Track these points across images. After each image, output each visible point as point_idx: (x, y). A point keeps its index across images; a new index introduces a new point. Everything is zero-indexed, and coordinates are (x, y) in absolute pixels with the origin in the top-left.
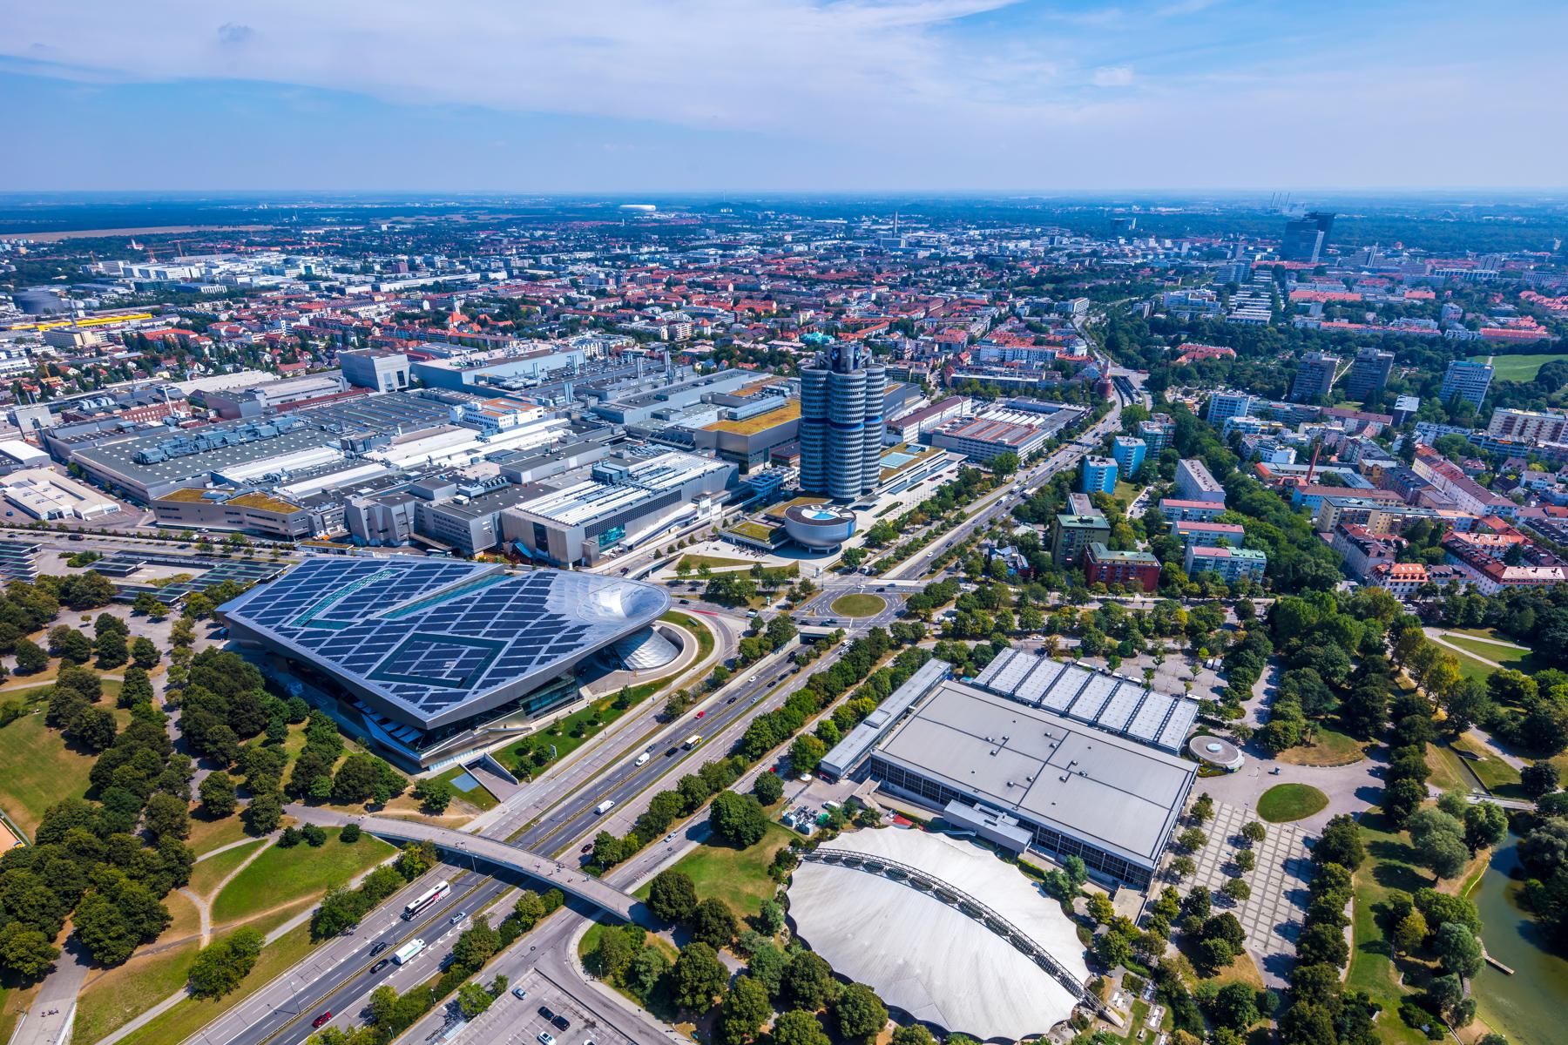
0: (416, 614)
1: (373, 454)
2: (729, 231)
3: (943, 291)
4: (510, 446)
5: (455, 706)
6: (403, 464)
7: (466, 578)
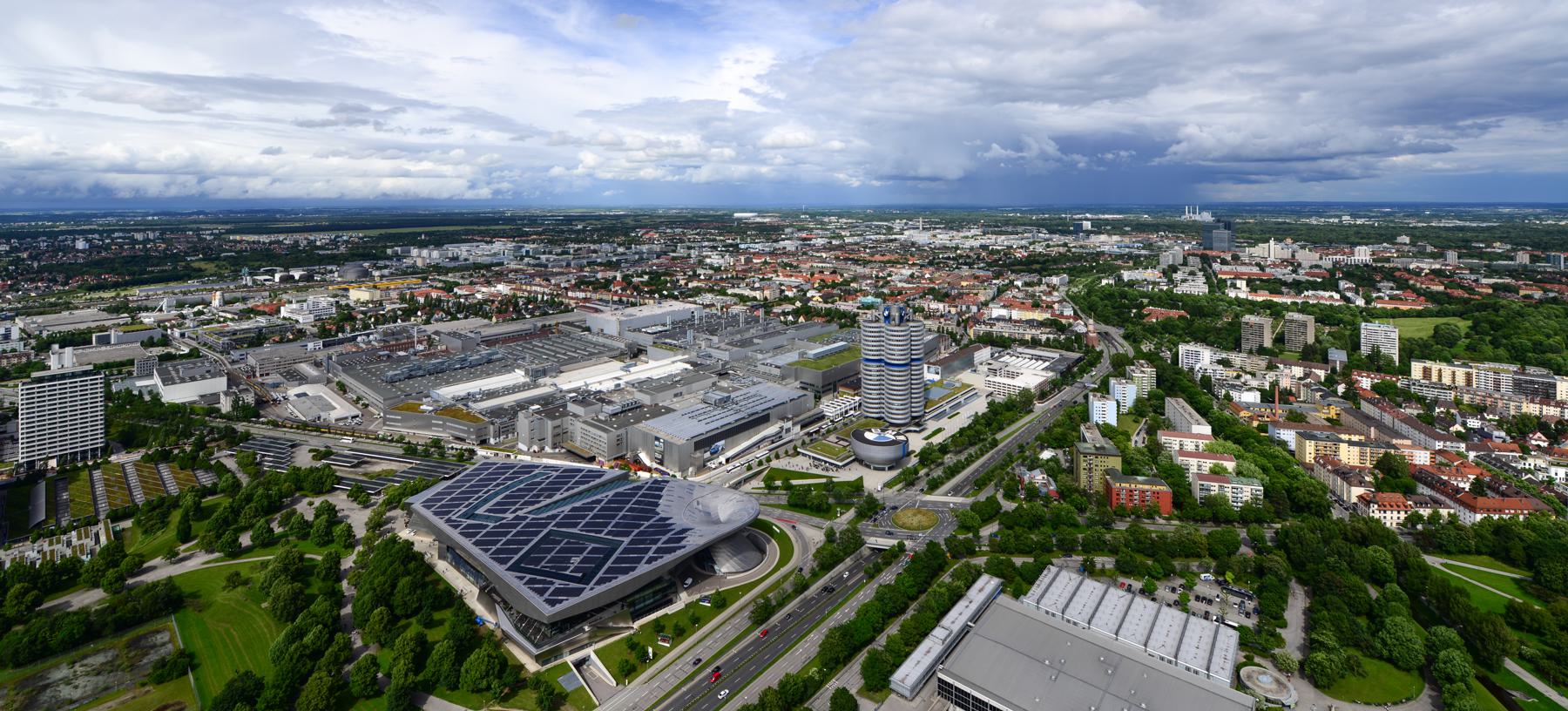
0: (554, 512)
1: (547, 380)
4: (643, 376)
5: (573, 601)
6: (565, 387)
7: (598, 481)
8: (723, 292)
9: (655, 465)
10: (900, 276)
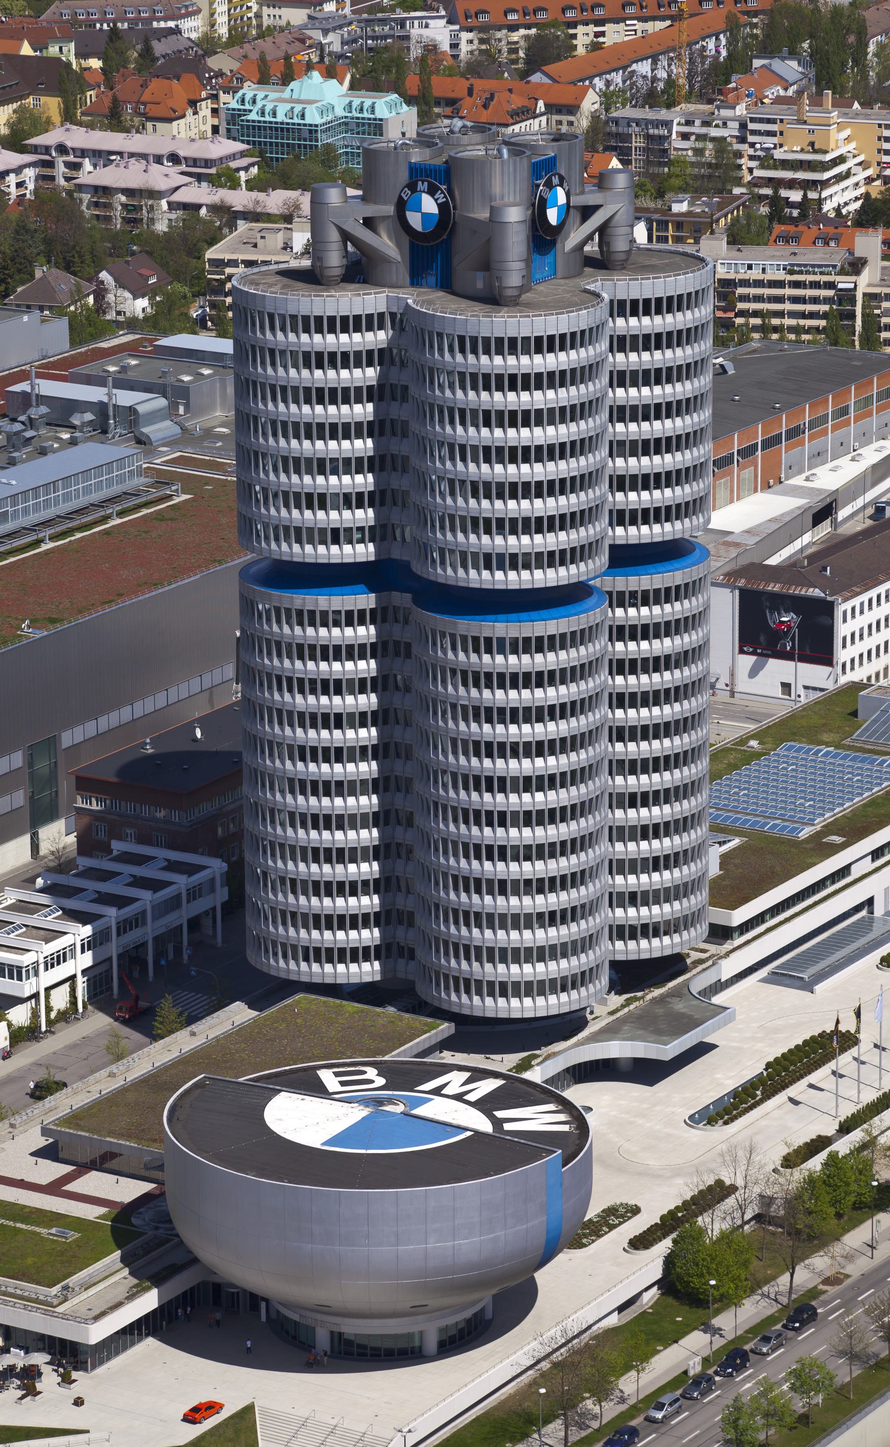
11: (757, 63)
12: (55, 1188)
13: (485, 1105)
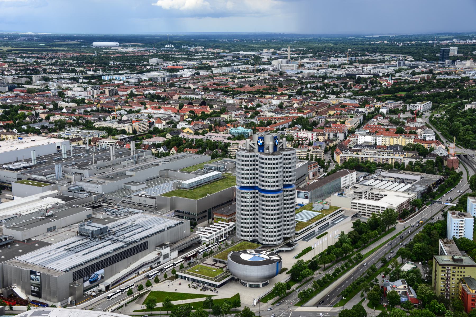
2: (173, 59)
3: (327, 98)
8: (88, 126)
9: (32, 298)
10: (269, 107)
11: (296, 126)
12: (213, 265)
13: (268, 255)
